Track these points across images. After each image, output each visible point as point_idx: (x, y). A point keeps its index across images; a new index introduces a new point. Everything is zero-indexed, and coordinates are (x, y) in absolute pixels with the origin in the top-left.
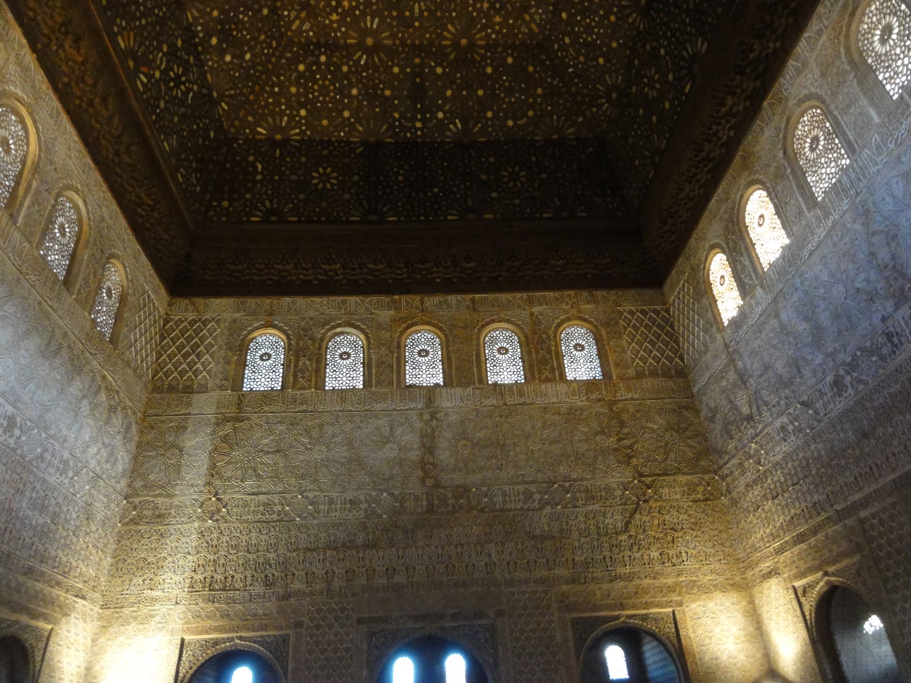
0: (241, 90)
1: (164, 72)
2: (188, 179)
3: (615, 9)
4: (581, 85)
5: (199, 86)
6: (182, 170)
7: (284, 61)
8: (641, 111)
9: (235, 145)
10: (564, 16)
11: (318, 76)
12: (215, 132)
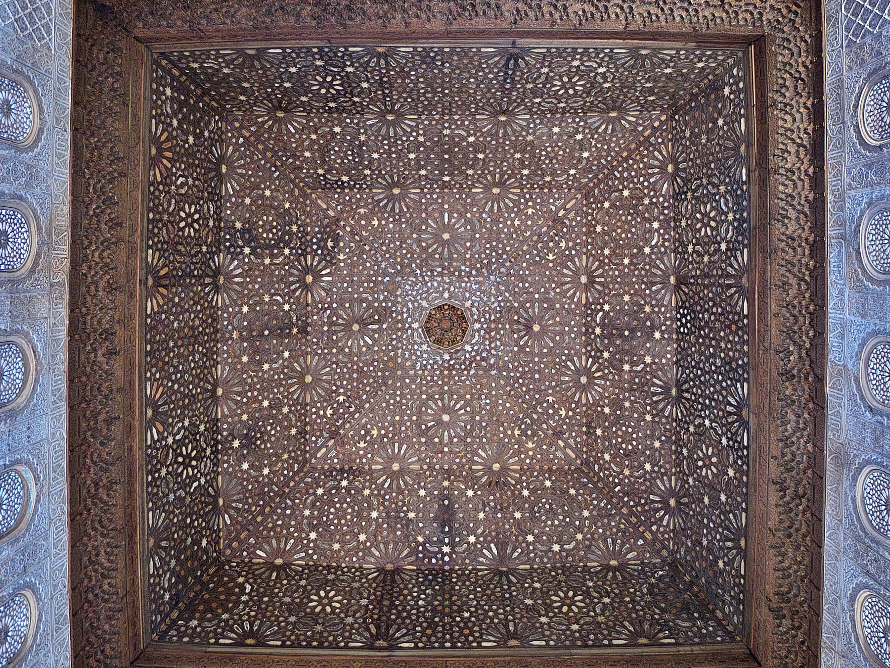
0: (250, 505)
1: (180, 443)
2: (160, 576)
3: (648, 408)
4: (632, 503)
5: (207, 481)
6: (157, 558)
7: (302, 485)
8: (706, 500)
9: (227, 567)
10: (599, 432)
11: (336, 500)
12: (208, 543)
